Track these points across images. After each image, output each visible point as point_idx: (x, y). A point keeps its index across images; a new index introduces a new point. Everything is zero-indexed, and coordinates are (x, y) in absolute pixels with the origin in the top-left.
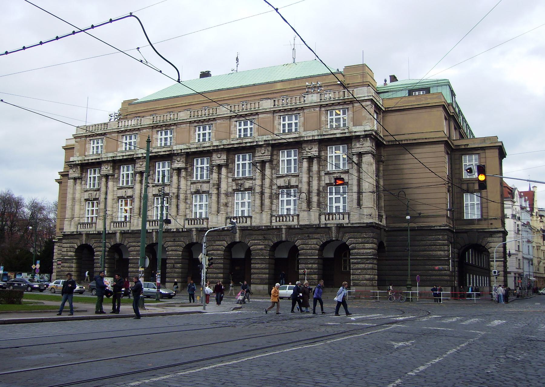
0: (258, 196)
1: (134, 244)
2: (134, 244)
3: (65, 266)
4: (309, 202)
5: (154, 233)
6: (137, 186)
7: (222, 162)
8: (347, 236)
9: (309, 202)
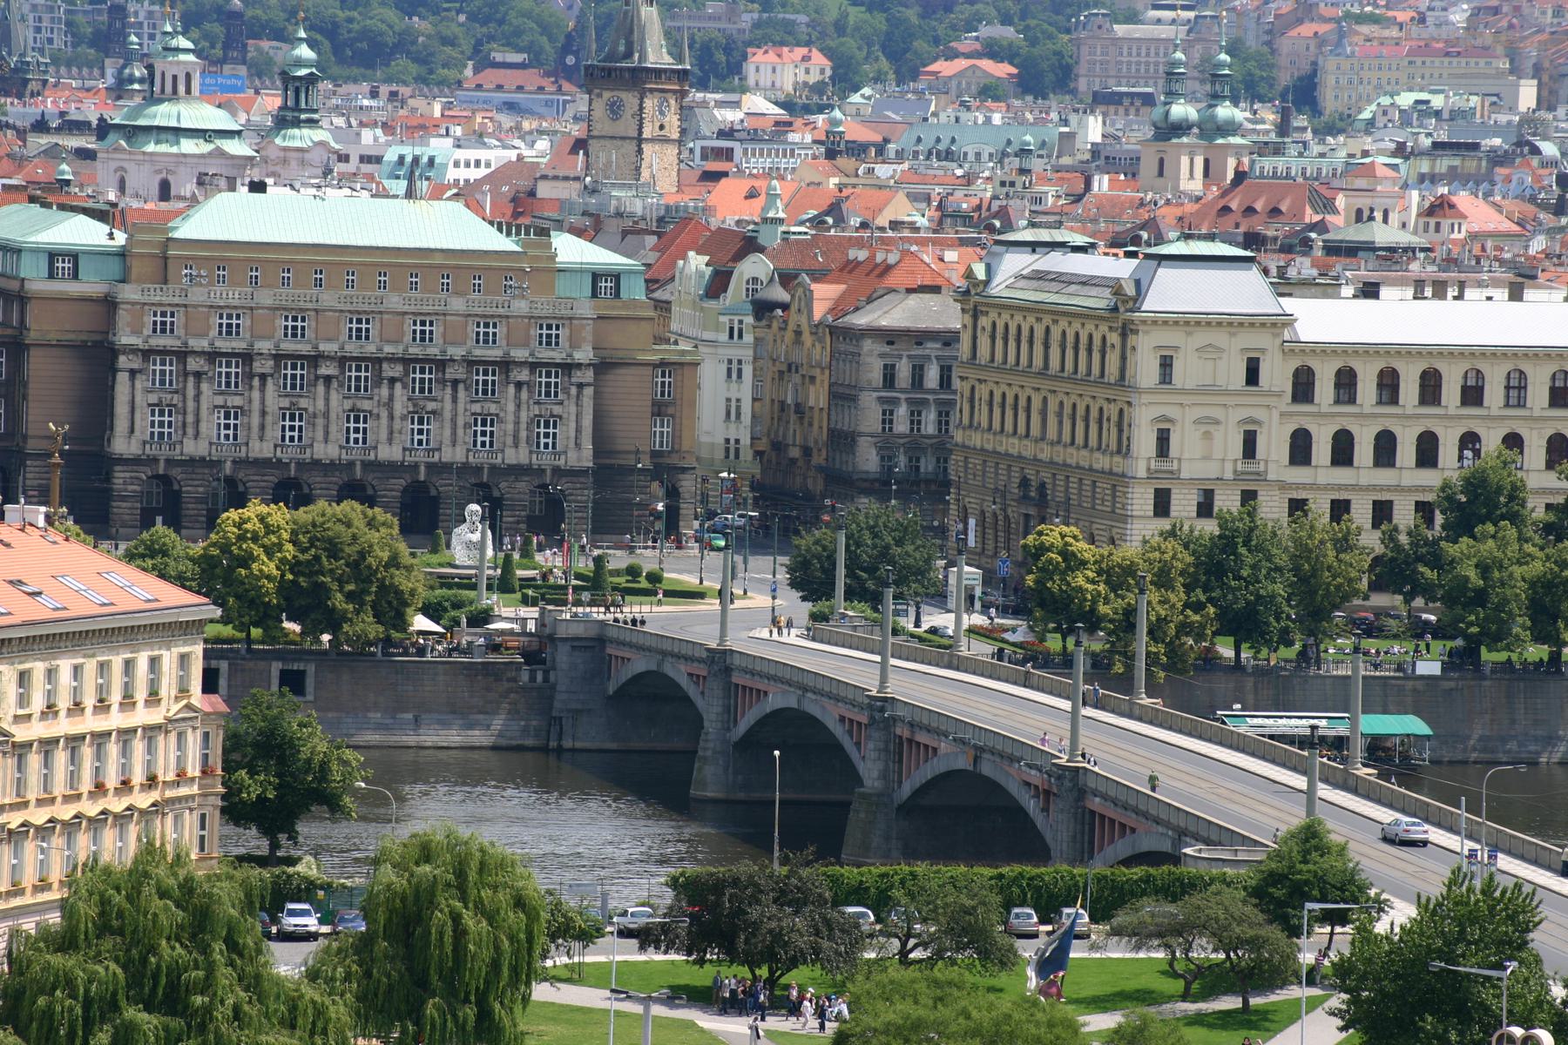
0: (448, 425)
4: (516, 437)
6: (256, 395)
7: (397, 375)
9: (516, 437)
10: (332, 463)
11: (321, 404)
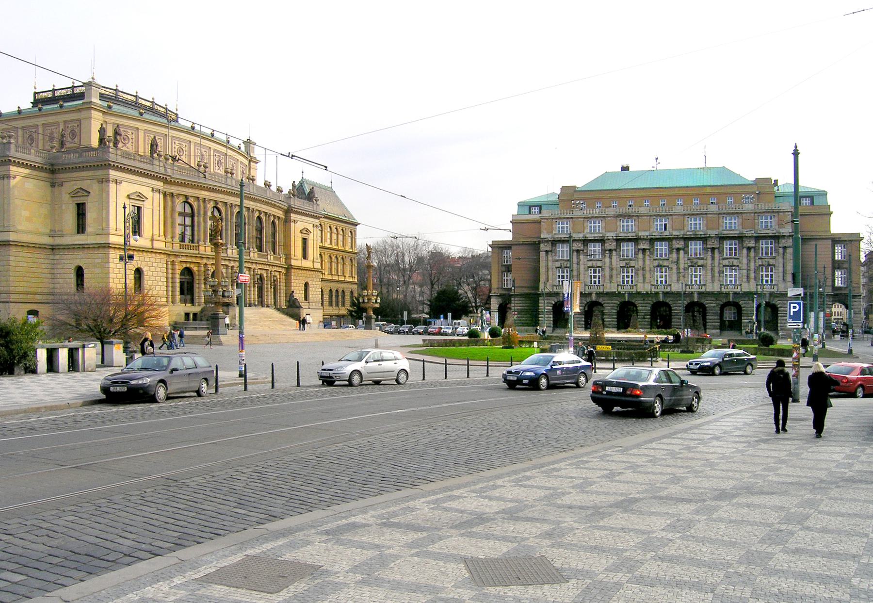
1: (608, 301)
2: (608, 301)
4: (748, 277)
5: (627, 295)
6: (607, 260)
7: (680, 247)
8: (777, 299)
9: (748, 277)
10: (647, 293)
11: (641, 263)
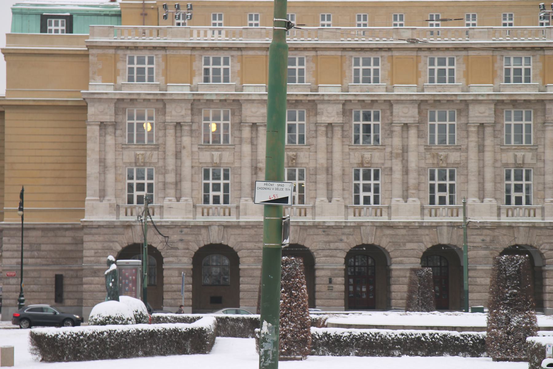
3: (95, 282)
11: (322, 158)
